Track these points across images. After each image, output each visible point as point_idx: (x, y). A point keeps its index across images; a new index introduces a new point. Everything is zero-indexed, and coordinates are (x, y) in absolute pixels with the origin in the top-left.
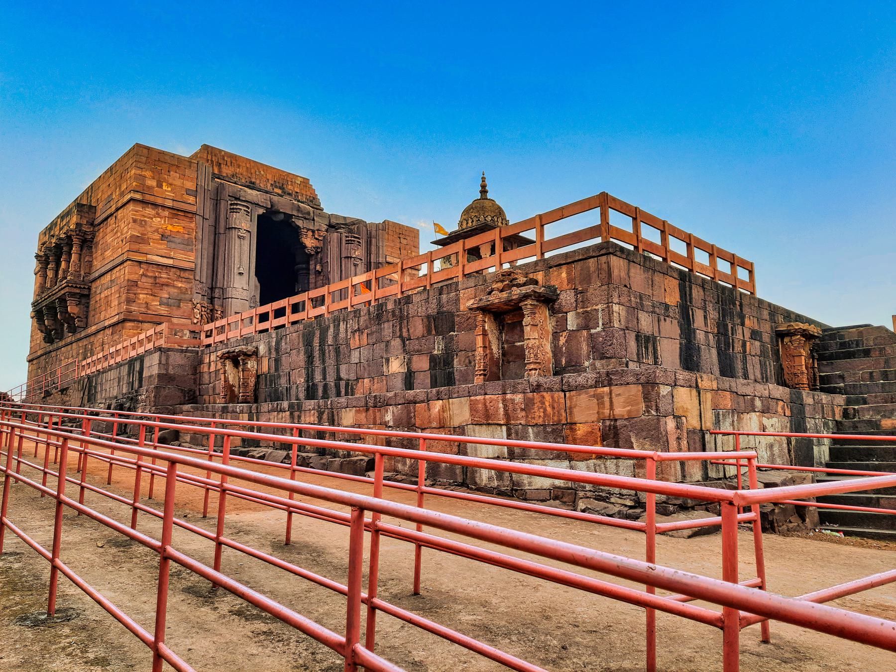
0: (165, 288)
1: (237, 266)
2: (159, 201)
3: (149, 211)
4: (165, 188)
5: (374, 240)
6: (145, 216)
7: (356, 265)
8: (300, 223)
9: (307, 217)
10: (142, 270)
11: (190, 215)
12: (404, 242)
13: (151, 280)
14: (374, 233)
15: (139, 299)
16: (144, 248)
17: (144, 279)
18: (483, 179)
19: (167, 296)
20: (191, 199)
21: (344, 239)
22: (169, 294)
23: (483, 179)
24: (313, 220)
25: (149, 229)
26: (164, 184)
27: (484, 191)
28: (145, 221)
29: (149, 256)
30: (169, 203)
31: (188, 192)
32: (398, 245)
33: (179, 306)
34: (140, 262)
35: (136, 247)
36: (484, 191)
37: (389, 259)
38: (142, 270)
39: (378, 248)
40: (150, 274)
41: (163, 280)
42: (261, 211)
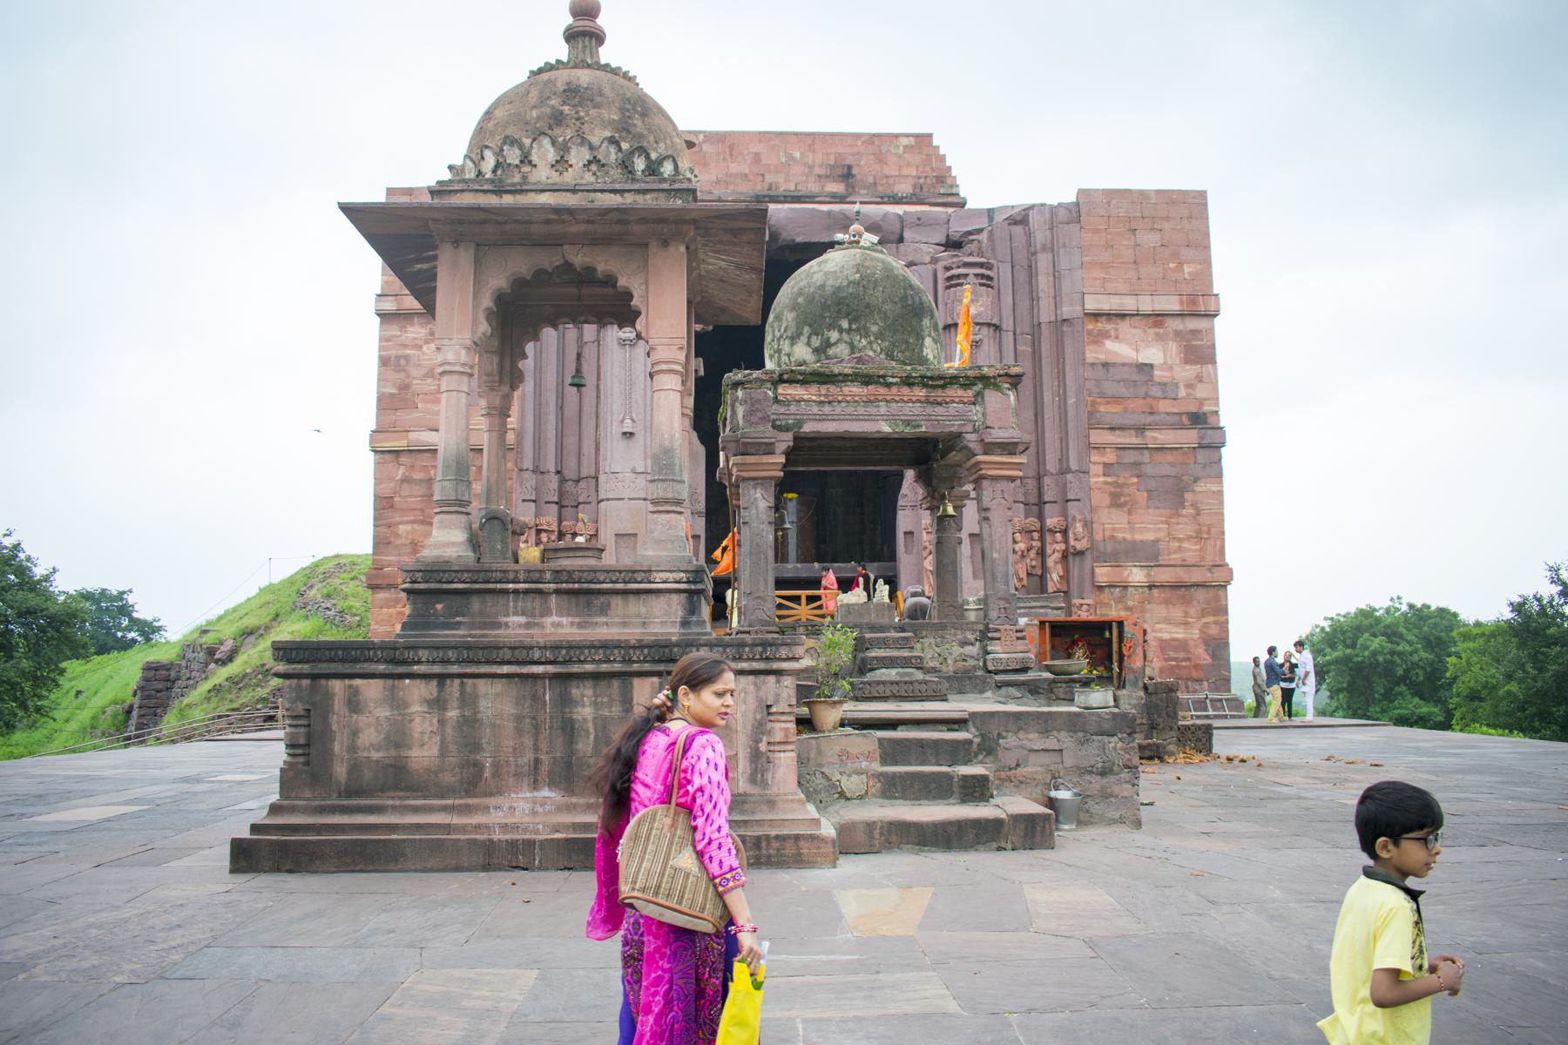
1: (617, 417)
5: (1043, 261)
6: (405, 346)
10: (402, 470)
12: (1150, 240)
13: (420, 490)
14: (1040, 237)
15: (397, 535)
16: (405, 417)
17: (406, 490)
21: (941, 276)
24: (901, 240)
25: (414, 372)
27: (584, 33)
28: (407, 358)
29: (412, 436)
32: (1128, 254)
34: (396, 453)
35: (391, 417)
36: (584, 33)
37: (1092, 304)
38: (402, 470)
39: (1056, 275)
40: (418, 476)
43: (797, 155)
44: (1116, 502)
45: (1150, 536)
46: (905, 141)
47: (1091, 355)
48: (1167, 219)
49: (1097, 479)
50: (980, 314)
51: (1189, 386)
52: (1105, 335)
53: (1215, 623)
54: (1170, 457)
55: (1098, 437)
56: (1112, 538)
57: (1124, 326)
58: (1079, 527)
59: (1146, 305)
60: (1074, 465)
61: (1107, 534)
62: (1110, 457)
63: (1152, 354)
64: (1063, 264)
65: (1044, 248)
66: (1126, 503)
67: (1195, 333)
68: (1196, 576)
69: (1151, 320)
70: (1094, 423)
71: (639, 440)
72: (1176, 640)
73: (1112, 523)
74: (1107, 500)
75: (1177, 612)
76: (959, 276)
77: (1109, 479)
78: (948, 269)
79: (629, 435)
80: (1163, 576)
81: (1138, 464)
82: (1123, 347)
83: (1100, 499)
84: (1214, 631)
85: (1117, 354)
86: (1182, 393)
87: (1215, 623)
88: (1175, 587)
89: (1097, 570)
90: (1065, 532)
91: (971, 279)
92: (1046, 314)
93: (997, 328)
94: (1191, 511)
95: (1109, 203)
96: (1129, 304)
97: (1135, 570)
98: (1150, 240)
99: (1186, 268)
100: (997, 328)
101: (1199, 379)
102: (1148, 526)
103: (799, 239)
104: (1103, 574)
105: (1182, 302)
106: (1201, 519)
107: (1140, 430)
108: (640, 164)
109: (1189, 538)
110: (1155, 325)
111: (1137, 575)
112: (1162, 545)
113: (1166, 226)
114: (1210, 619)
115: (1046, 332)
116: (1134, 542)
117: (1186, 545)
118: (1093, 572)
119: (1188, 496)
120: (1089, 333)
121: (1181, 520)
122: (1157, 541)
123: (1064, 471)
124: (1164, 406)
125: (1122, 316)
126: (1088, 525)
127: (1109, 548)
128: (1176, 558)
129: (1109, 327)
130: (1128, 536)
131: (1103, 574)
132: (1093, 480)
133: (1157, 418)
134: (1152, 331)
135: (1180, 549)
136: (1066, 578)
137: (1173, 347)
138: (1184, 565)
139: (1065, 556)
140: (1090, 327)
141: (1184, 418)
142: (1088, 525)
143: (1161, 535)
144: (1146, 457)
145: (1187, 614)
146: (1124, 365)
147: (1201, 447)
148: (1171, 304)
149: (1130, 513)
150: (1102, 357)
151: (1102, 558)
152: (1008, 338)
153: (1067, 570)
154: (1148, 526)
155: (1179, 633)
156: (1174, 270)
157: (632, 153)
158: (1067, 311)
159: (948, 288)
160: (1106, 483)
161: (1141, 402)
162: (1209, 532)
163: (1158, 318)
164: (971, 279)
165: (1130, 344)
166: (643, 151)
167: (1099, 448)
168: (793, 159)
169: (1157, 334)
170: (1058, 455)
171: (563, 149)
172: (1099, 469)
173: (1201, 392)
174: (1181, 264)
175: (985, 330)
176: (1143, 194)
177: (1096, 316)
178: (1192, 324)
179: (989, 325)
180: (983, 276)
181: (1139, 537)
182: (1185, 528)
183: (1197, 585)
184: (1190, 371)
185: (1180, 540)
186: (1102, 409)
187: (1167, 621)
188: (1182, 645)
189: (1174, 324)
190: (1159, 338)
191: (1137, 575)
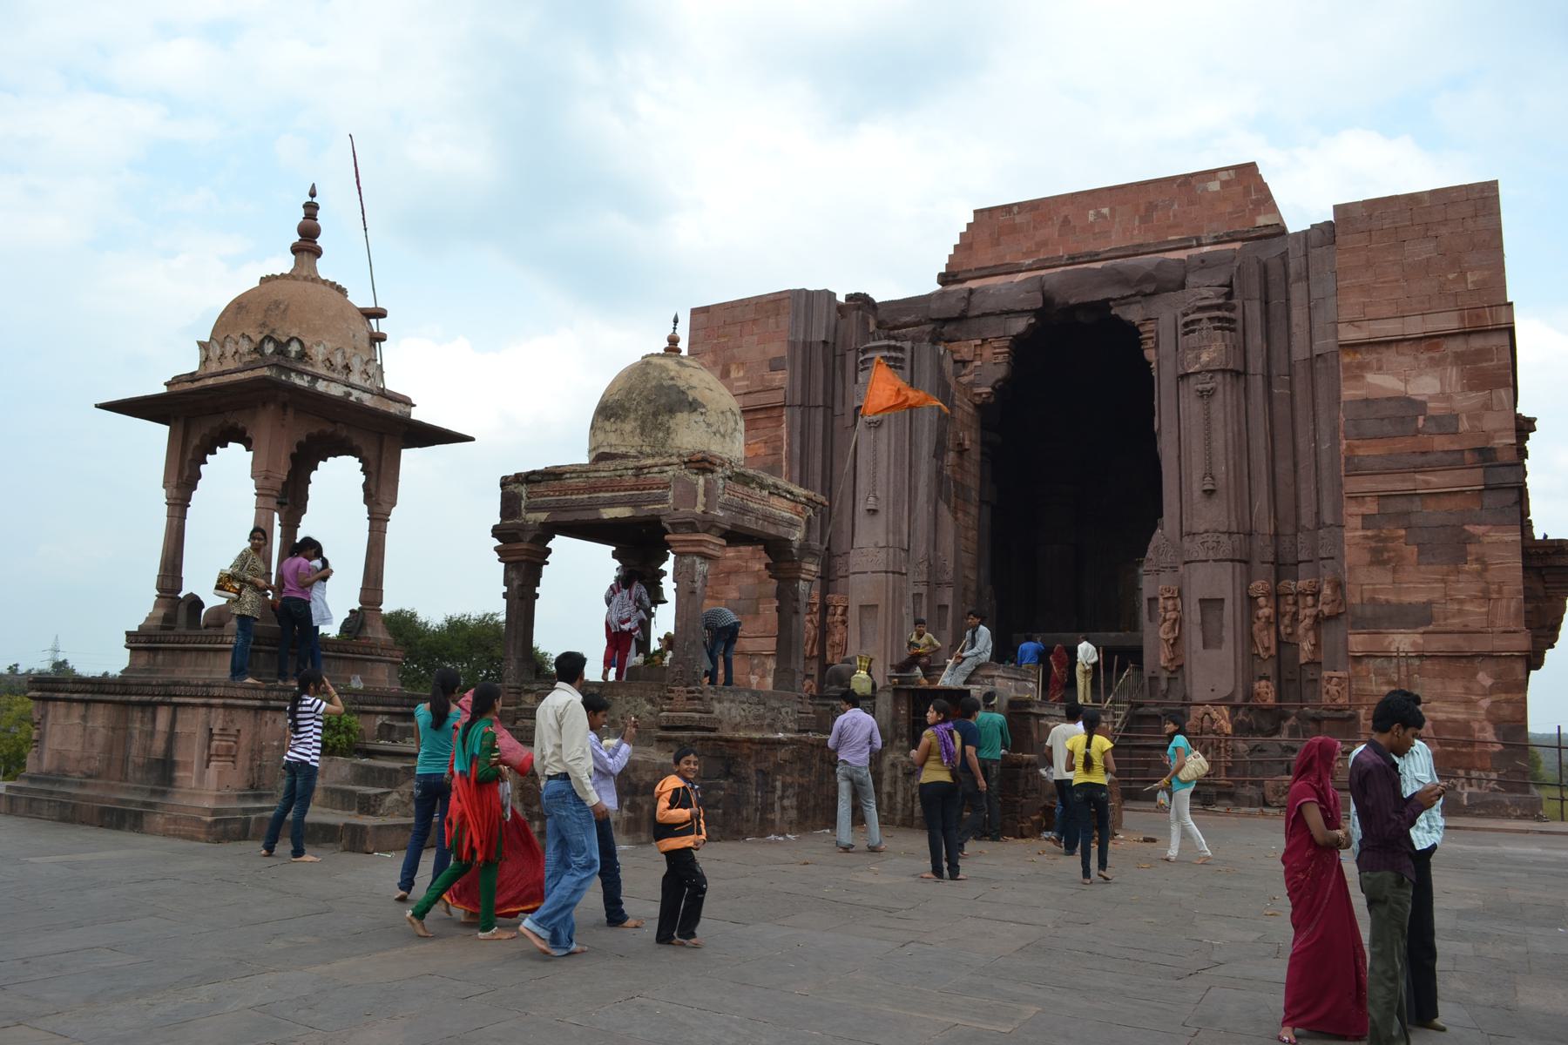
0: (732, 578)
4: (733, 375)
5: (1297, 292)
7: (1206, 395)
8: (1133, 314)
9: (1150, 288)
11: (775, 413)
18: (311, 209)
19: (734, 595)
20: (780, 378)
22: (740, 589)
23: (311, 209)
26: (733, 367)
31: (775, 365)
33: (757, 613)
37: (1349, 334)
41: (728, 563)
42: (1019, 325)
43: (1105, 211)
44: (1378, 558)
45: (1420, 598)
46: (1224, 176)
47: (1349, 392)
48: (1445, 222)
49: (1354, 532)
50: (1213, 360)
51: (1474, 416)
52: (1363, 367)
53: (1508, 701)
54: (1449, 504)
55: (1353, 485)
56: (1373, 600)
57: (1389, 355)
58: (1327, 591)
59: (1415, 327)
60: (1328, 518)
61: (1366, 596)
62: (1371, 507)
63: (1425, 386)
64: (1316, 293)
65: (1299, 279)
66: (1389, 560)
67: (1482, 354)
68: (1479, 645)
69: (1424, 344)
70: (1355, 469)
71: (882, 516)
72: (1455, 721)
74: (1367, 557)
75: (1456, 689)
76: (1193, 322)
77: (1369, 533)
78: (1185, 315)
79: (873, 512)
80: (1437, 644)
81: (1408, 513)
82: (1384, 381)
84: (1506, 711)
85: (1380, 387)
86: (1464, 425)
87: (1508, 701)
88: (1455, 657)
89: (1351, 638)
90: (1316, 594)
91: (1205, 324)
92: (1300, 352)
93: (1237, 374)
94: (1476, 566)
95: (1370, 216)
96: (1391, 328)
97: (1398, 637)
98: (1421, 251)
99: (1470, 278)
100: (1237, 374)
101: (1487, 407)
102: (1417, 586)
103: (1072, 301)
104: (1358, 642)
105: (1462, 319)
106: (1488, 576)
108: (269, 348)
109: (1473, 598)
110: (1429, 349)
112: (1436, 609)
113: (1444, 231)
114: (1503, 696)
115: (1301, 373)
116: (1400, 605)
117: (1468, 607)
118: (1346, 640)
119: (1470, 548)
120: (1347, 367)
121: (1462, 577)
122: (1430, 603)
123: (1319, 525)
124: (1441, 443)
125: (1388, 343)
126: (1338, 586)
127: (1368, 611)
128: (1455, 622)
129: (1371, 357)
130: (1393, 598)
131: (1358, 642)
132: (1347, 534)
133: (1430, 458)
134: (1424, 356)
135: (1460, 612)
136: (1316, 646)
137: (1453, 373)
138: (1465, 632)
139: (1318, 621)
140: (1346, 359)
141: (1468, 456)
142: (1338, 586)
143: (1436, 596)
144: (1416, 505)
145: (1468, 690)
146: (1389, 399)
147: (1489, 488)
148: (1449, 322)
149: (1394, 571)
150: (1361, 393)
151: (1360, 624)
152: (1257, 384)
153: (1317, 637)
154: (1417, 586)
155: (1460, 714)
156: (1454, 281)
157: (262, 342)
158: (1320, 345)
159: (1186, 334)
160: (1366, 537)
161: (1410, 441)
162: (1500, 591)
163: (1431, 340)
164: (1205, 324)
165: (1396, 375)
166: (269, 338)
167: (1357, 498)
168: (1104, 217)
169: (1431, 359)
170: (1314, 509)
171: (223, 346)
172: (1358, 522)
174: (1463, 274)
175: (1219, 377)
176: (1413, 199)
177: (1354, 347)
178: (1477, 343)
179: (1224, 371)
180: (1220, 319)
181: (1406, 599)
182: (1465, 586)
184: (1477, 398)
185: (1461, 602)
186: (1361, 452)
187: (1443, 698)
188: (1465, 727)
189: (1457, 345)
190: (1434, 363)
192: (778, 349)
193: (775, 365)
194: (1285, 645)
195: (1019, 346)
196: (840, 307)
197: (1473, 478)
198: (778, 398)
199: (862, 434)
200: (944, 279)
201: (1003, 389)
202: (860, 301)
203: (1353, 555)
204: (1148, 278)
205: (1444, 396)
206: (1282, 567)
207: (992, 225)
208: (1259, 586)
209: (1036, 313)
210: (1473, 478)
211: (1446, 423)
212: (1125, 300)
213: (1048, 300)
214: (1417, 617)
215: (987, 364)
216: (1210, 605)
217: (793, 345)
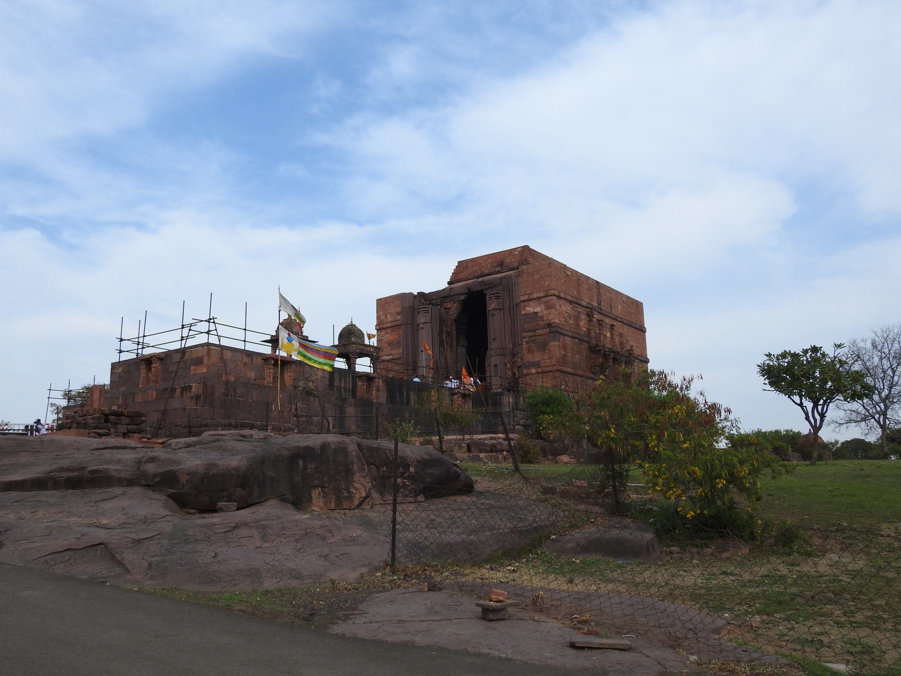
2: (385, 326)
3: (383, 333)
20: (399, 317)
30: (389, 325)
31: (398, 314)
37: (522, 298)
42: (462, 297)
44: (529, 351)
47: (523, 313)
51: (547, 316)
62: (527, 339)
63: (538, 309)
67: (548, 301)
68: (548, 369)
70: (524, 331)
73: (529, 358)
80: (540, 370)
82: (530, 309)
83: (525, 351)
98: (536, 277)
102: (537, 357)
104: (525, 371)
107: (534, 331)
111: (534, 371)
124: (541, 323)
126: (522, 359)
142: (522, 359)
148: (542, 294)
154: (537, 357)
163: (539, 298)
173: (550, 317)
177: (524, 301)
178: (548, 298)
182: (546, 356)
183: (550, 371)
184: (547, 312)
189: (544, 299)
190: (540, 304)
191: (534, 371)
192: (398, 309)
193: (398, 314)
194: (514, 374)
195: (464, 303)
196: (415, 297)
197: (547, 331)
198: (399, 323)
199: (421, 332)
200: (449, 283)
201: (461, 314)
202: (421, 295)
203: (525, 351)
204: (490, 283)
205: (541, 312)
206: (513, 356)
207: (462, 267)
208: (506, 361)
209: (467, 294)
210: (547, 331)
211: (542, 318)
212: (487, 289)
213: (469, 290)
214: (537, 365)
215: (454, 308)
216: (496, 366)
217: (402, 308)
